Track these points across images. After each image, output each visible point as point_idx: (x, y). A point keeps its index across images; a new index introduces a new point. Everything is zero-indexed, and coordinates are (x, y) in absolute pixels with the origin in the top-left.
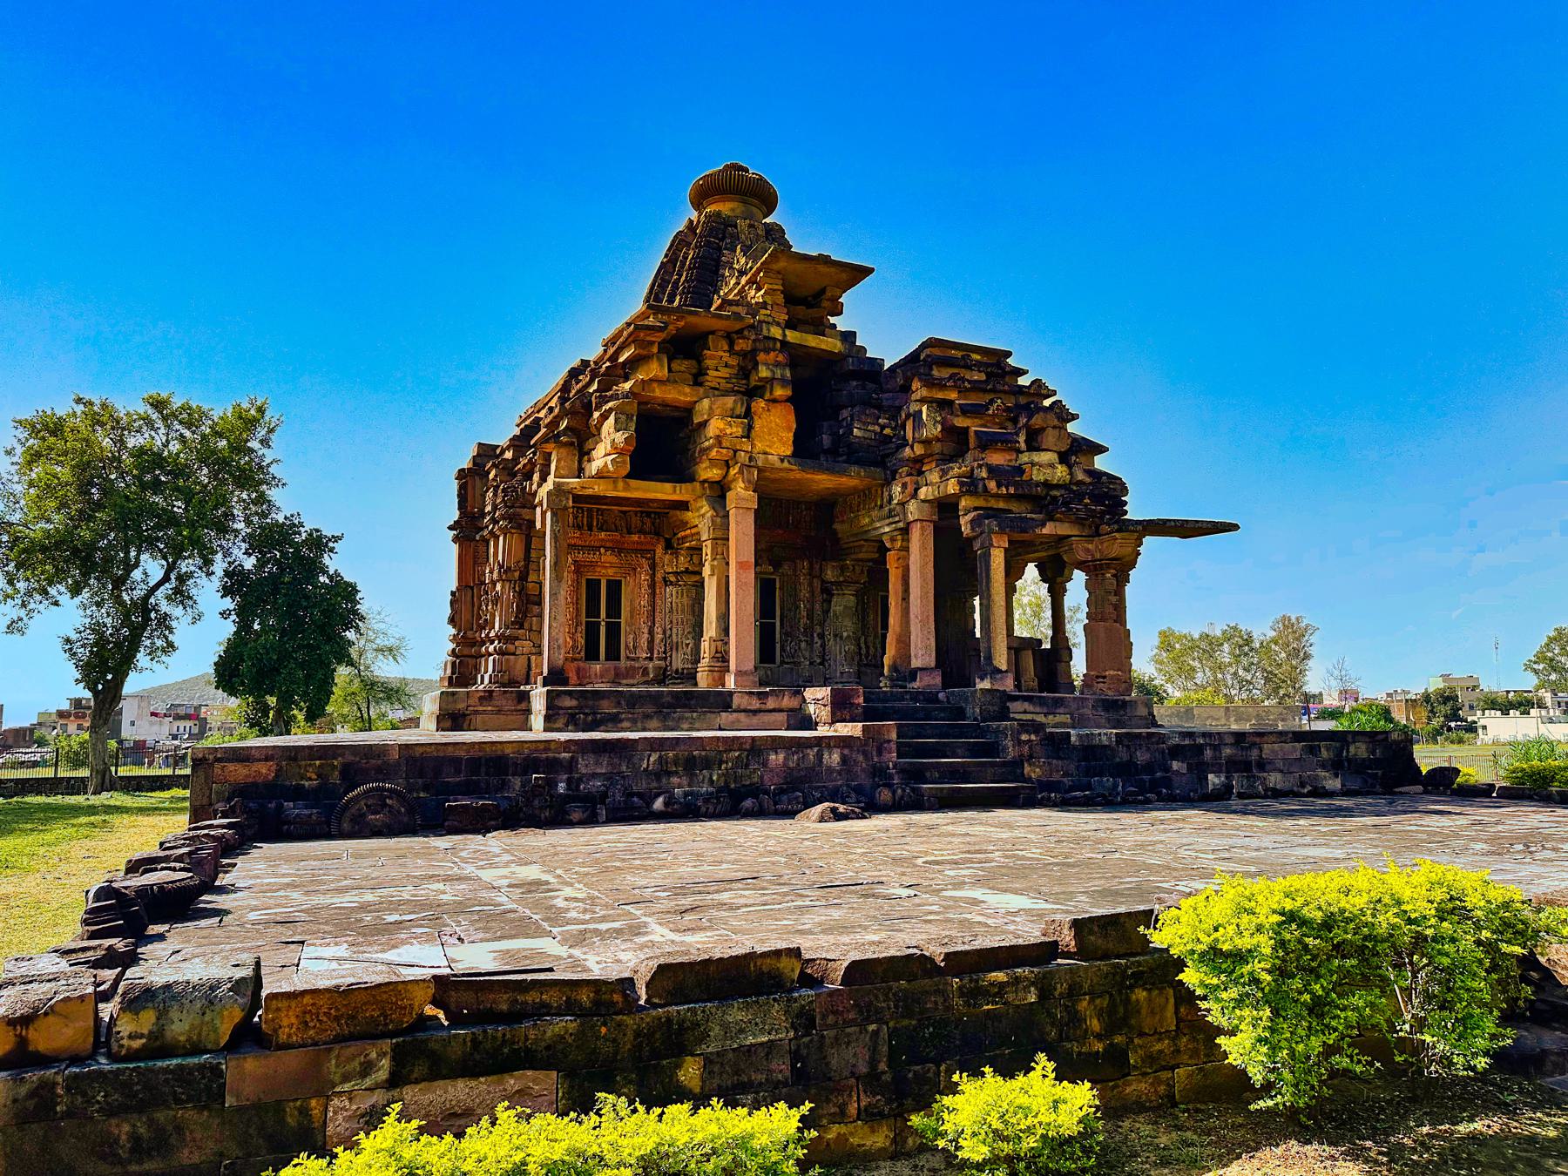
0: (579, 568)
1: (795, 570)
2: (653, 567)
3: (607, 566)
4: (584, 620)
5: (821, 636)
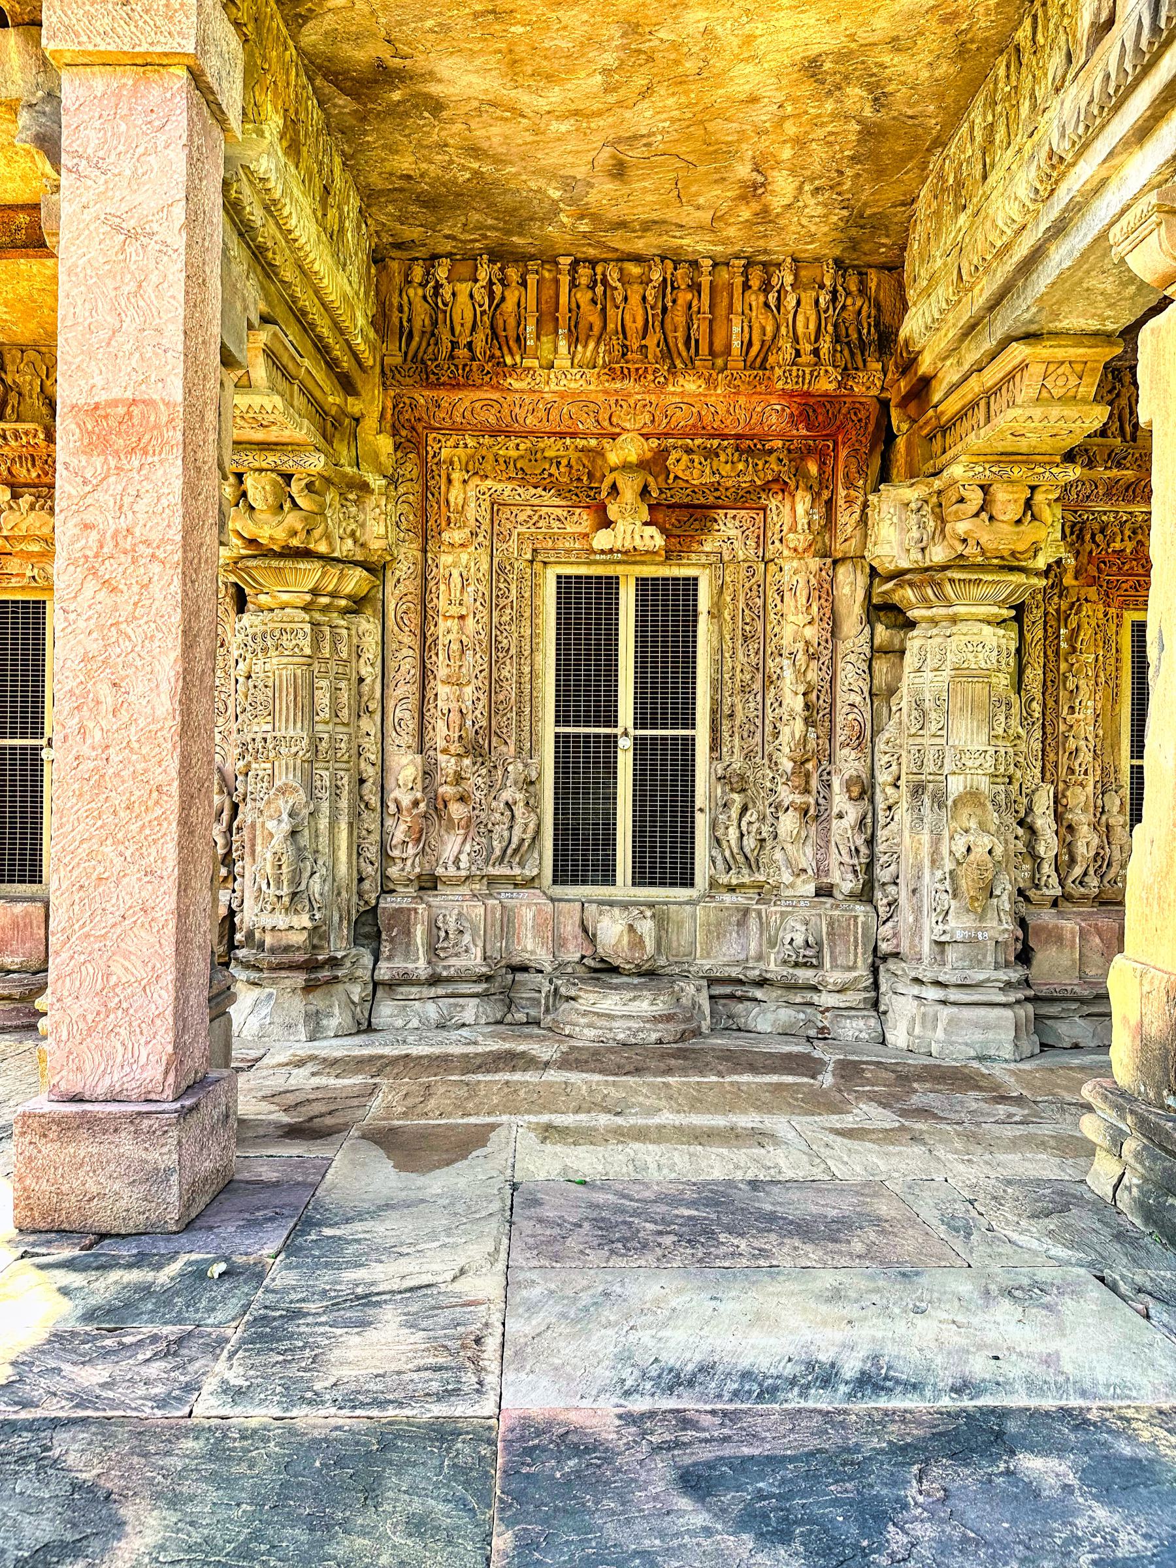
1: (762, 541)
5: (864, 790)
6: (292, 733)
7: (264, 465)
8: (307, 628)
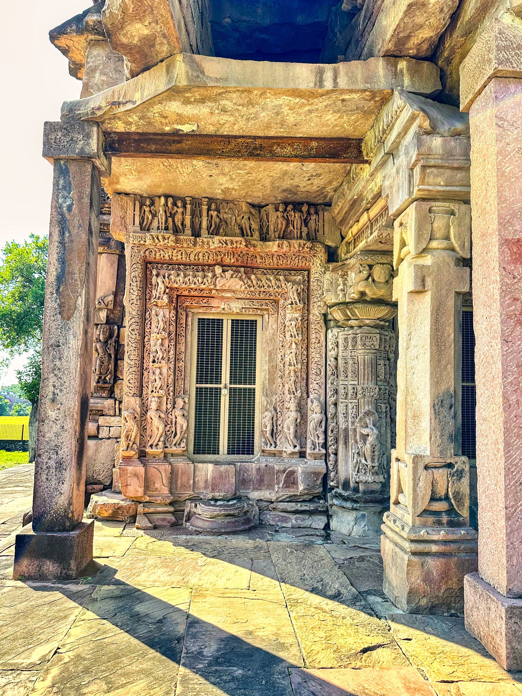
0: (177, 300)
2: (306, 297)
3: (229, 299)
4: (193, 385)
6: (371, 386)
7: (385, 261)
8: (378, 336)
